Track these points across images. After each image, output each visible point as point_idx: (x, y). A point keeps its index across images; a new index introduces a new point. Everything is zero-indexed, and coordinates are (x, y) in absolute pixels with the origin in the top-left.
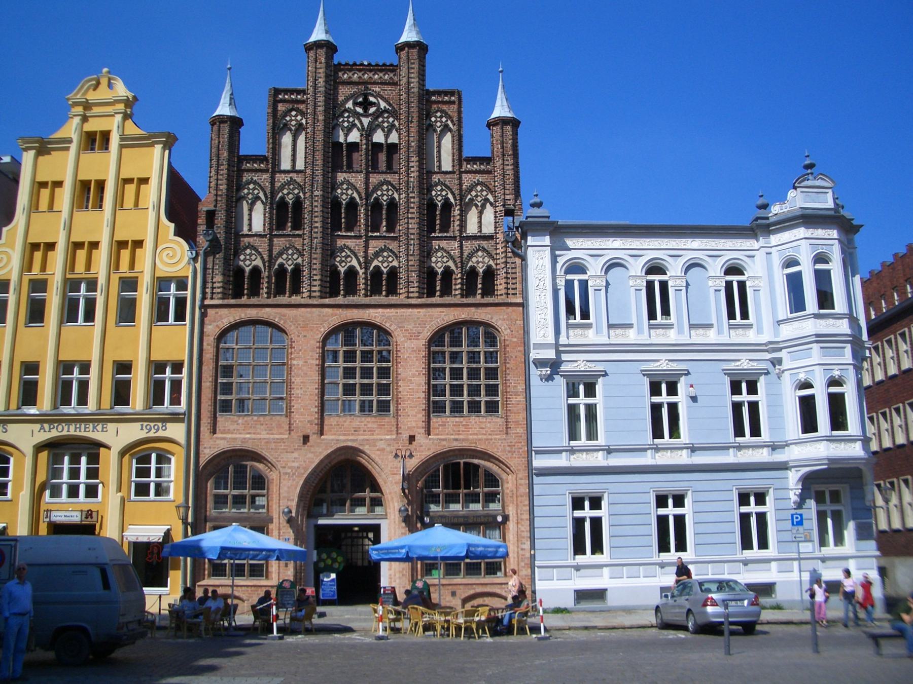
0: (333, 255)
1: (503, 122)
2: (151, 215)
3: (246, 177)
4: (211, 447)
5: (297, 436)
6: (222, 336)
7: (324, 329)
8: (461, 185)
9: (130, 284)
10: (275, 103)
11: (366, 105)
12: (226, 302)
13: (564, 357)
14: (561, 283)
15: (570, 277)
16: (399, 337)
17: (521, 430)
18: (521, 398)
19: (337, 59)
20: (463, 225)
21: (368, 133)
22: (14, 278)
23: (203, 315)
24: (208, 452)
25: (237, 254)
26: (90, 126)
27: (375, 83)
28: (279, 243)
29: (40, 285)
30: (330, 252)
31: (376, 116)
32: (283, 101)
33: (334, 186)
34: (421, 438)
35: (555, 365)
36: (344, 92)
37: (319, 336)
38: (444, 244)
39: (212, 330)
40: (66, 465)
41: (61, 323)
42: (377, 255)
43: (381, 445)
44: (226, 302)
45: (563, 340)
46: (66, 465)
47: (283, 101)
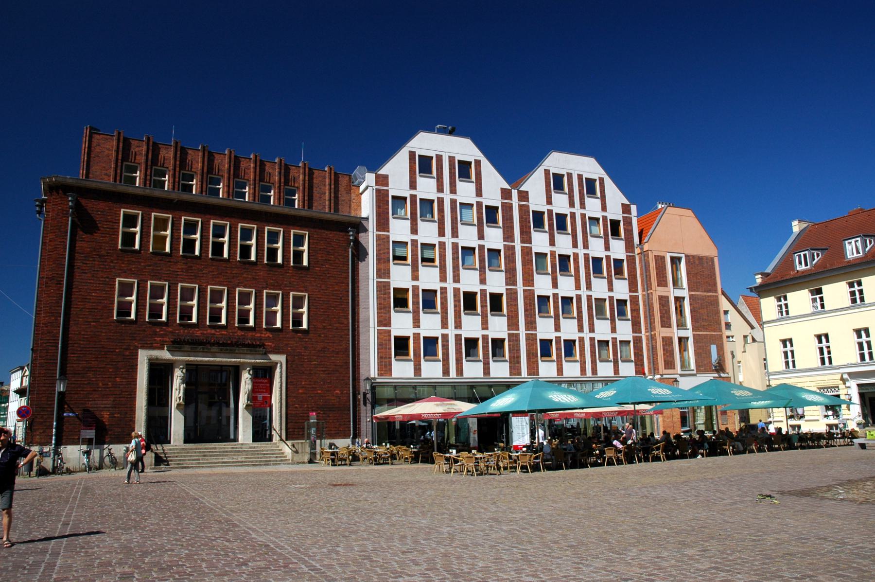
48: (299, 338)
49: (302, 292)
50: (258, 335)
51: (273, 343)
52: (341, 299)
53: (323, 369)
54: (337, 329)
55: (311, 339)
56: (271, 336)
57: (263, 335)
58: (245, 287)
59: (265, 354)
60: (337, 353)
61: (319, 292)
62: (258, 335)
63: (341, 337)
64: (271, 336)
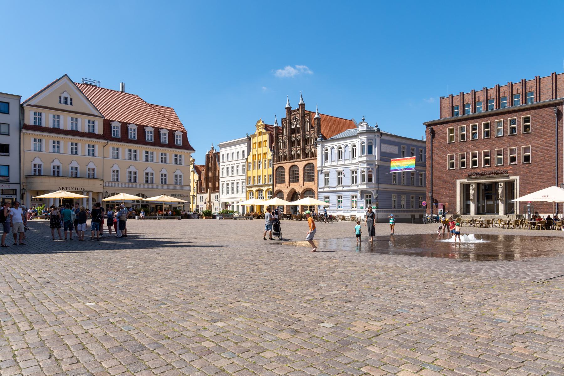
0: (291, 152)
1: (317, 118)
2: (267, 147)
3: (279, 138)
4: (276, 189)
5: (286, 187)
6: (276, 170)
7: (289, 167)
8: (310, 134)
9: (266, 161)
10: (282, 122)
11: (295, 119)
12: (277, 163)
13: (324, 169)
14: (324, 153)
15: (326, 151)
16: (299, 167)
17: (317, 184)
18: (317, 178)
19: (292, 109)
20: (311, 142)
21: (296, 126)
22: (251, 161)
23: (274, 166)
24: (275, 190)
25: (279, 153)
26: (259, 131)
27: (297, 114)
28: (284, 150)
29: (255, 162)
30: (291, 151)
31: (298, 120)
32: (284, 121)
33: (291, 138)
34: (302, 186)
35: (322, 171)
36: (292, 117)
37: (289, 168)
38: (308, 147)
39: (275, 168)
40: (260, 194)
41: (258, 169)
42: (298, 151)
43: (297, 188)
44: (277, 163)
45: (323, 165)
46: (260, 194)
47: (284, 121)
48: (527, 167)
49: (528, 145)
50: (506, 168)
51: (513, 171)
52: (551, 144)
53: (540, 181)
54: (549, 160)
55: (533, 167)
56: (512, 168)
57: (508, 168)
58: (499, 148)
59: (508, 176)
60: (549, 172)
61: (538, 143)
62: (506, 168)
63: (551, 164)
64: (512, 168)
